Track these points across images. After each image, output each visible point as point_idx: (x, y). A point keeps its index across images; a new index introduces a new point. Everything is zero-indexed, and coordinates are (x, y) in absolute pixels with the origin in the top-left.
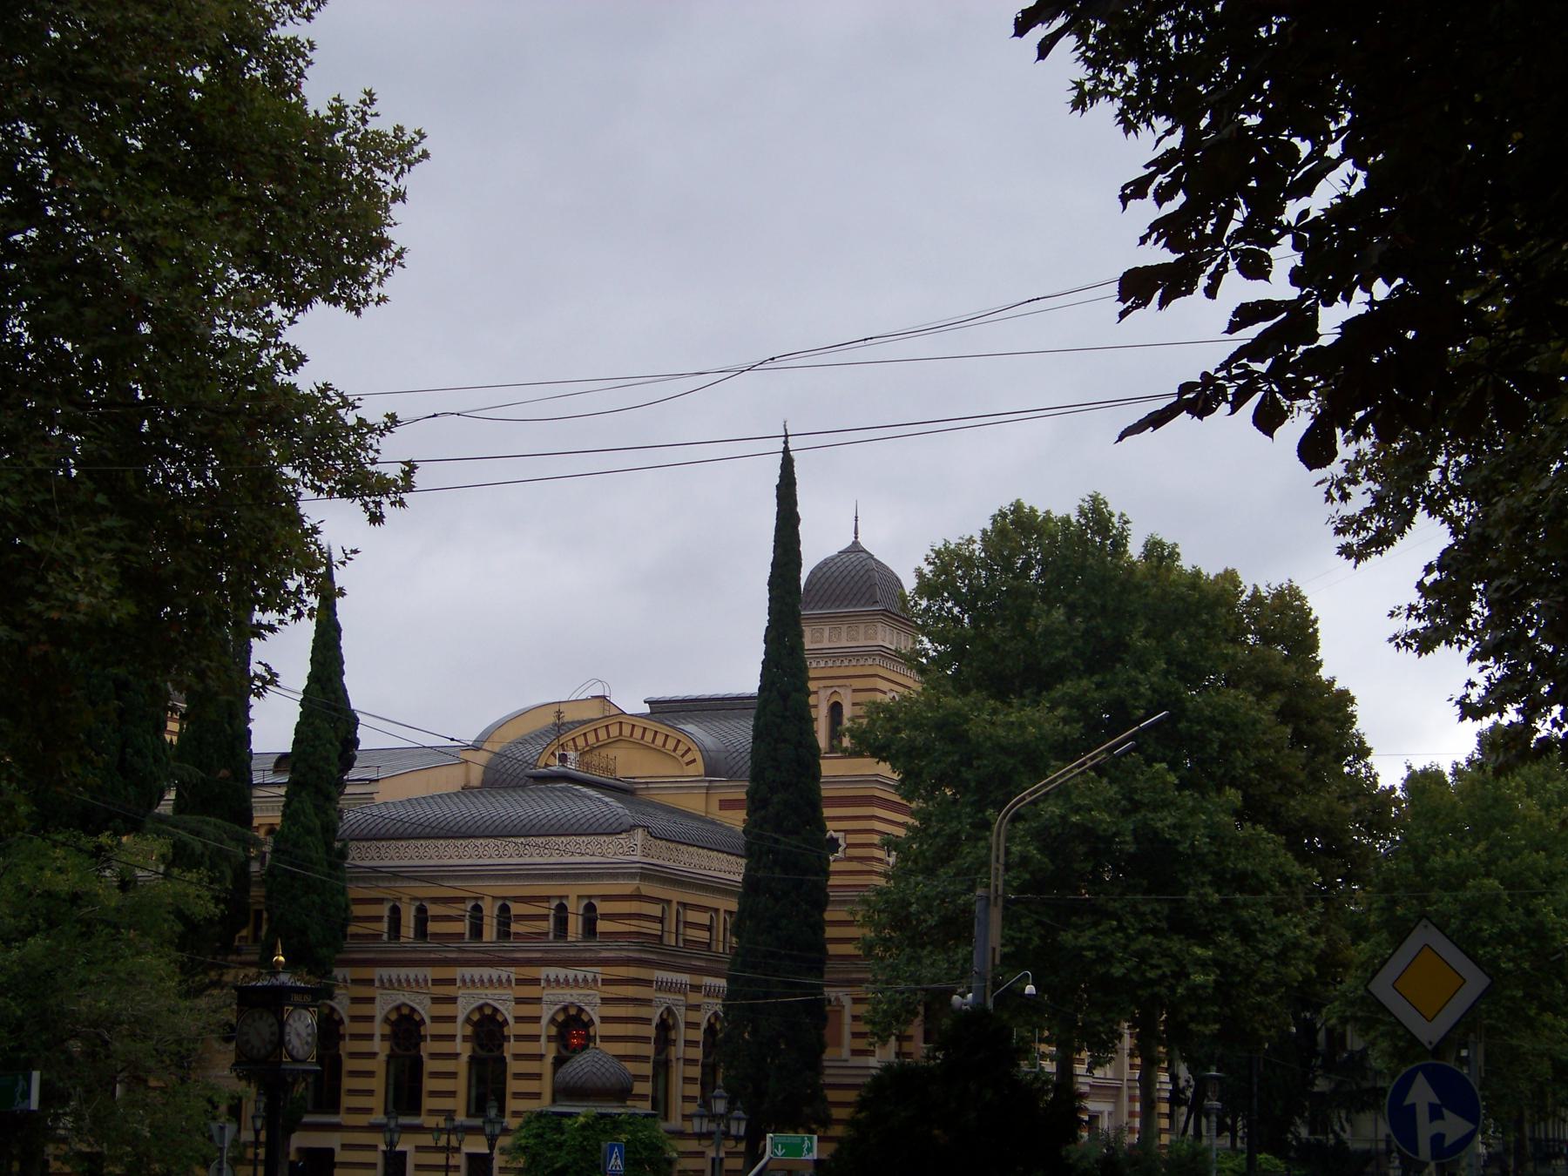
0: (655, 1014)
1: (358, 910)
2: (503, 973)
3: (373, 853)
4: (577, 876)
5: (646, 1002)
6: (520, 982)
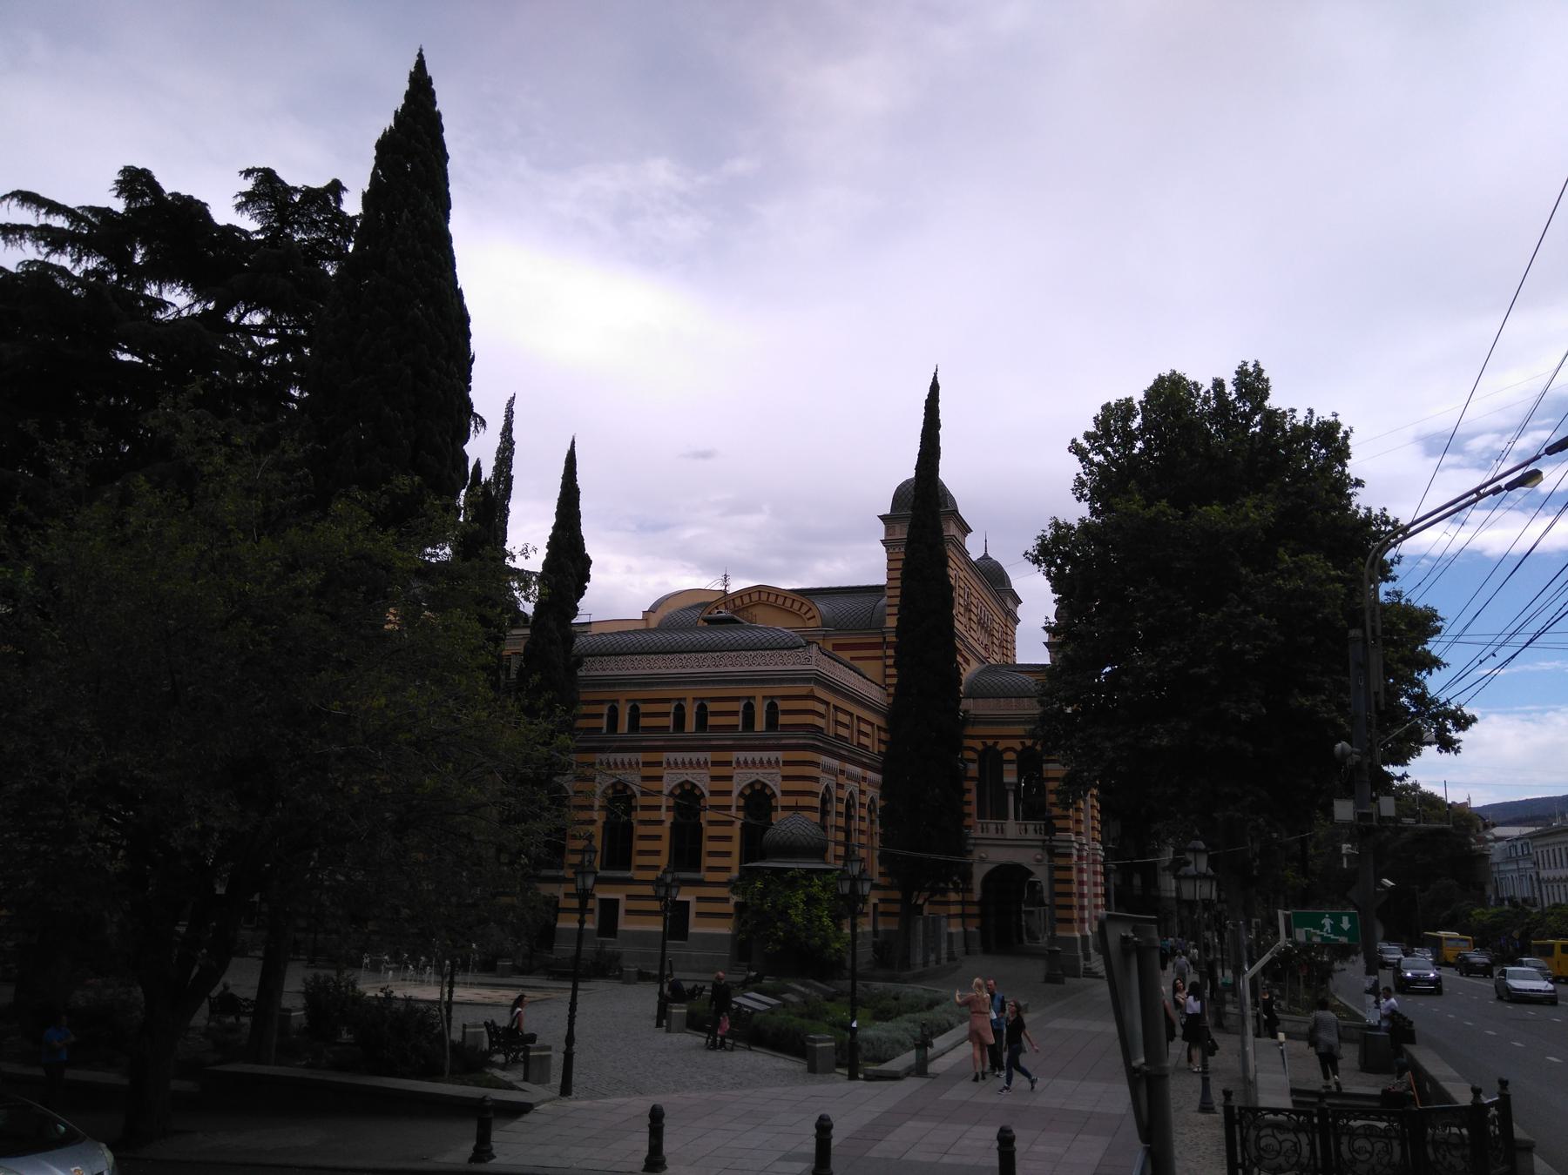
0: (821, 789)
1: (585, 709)
2: (774, 755)
3: (597, 666)
4: (763, 681)
5: (816, 780)
6: (714, 763)
